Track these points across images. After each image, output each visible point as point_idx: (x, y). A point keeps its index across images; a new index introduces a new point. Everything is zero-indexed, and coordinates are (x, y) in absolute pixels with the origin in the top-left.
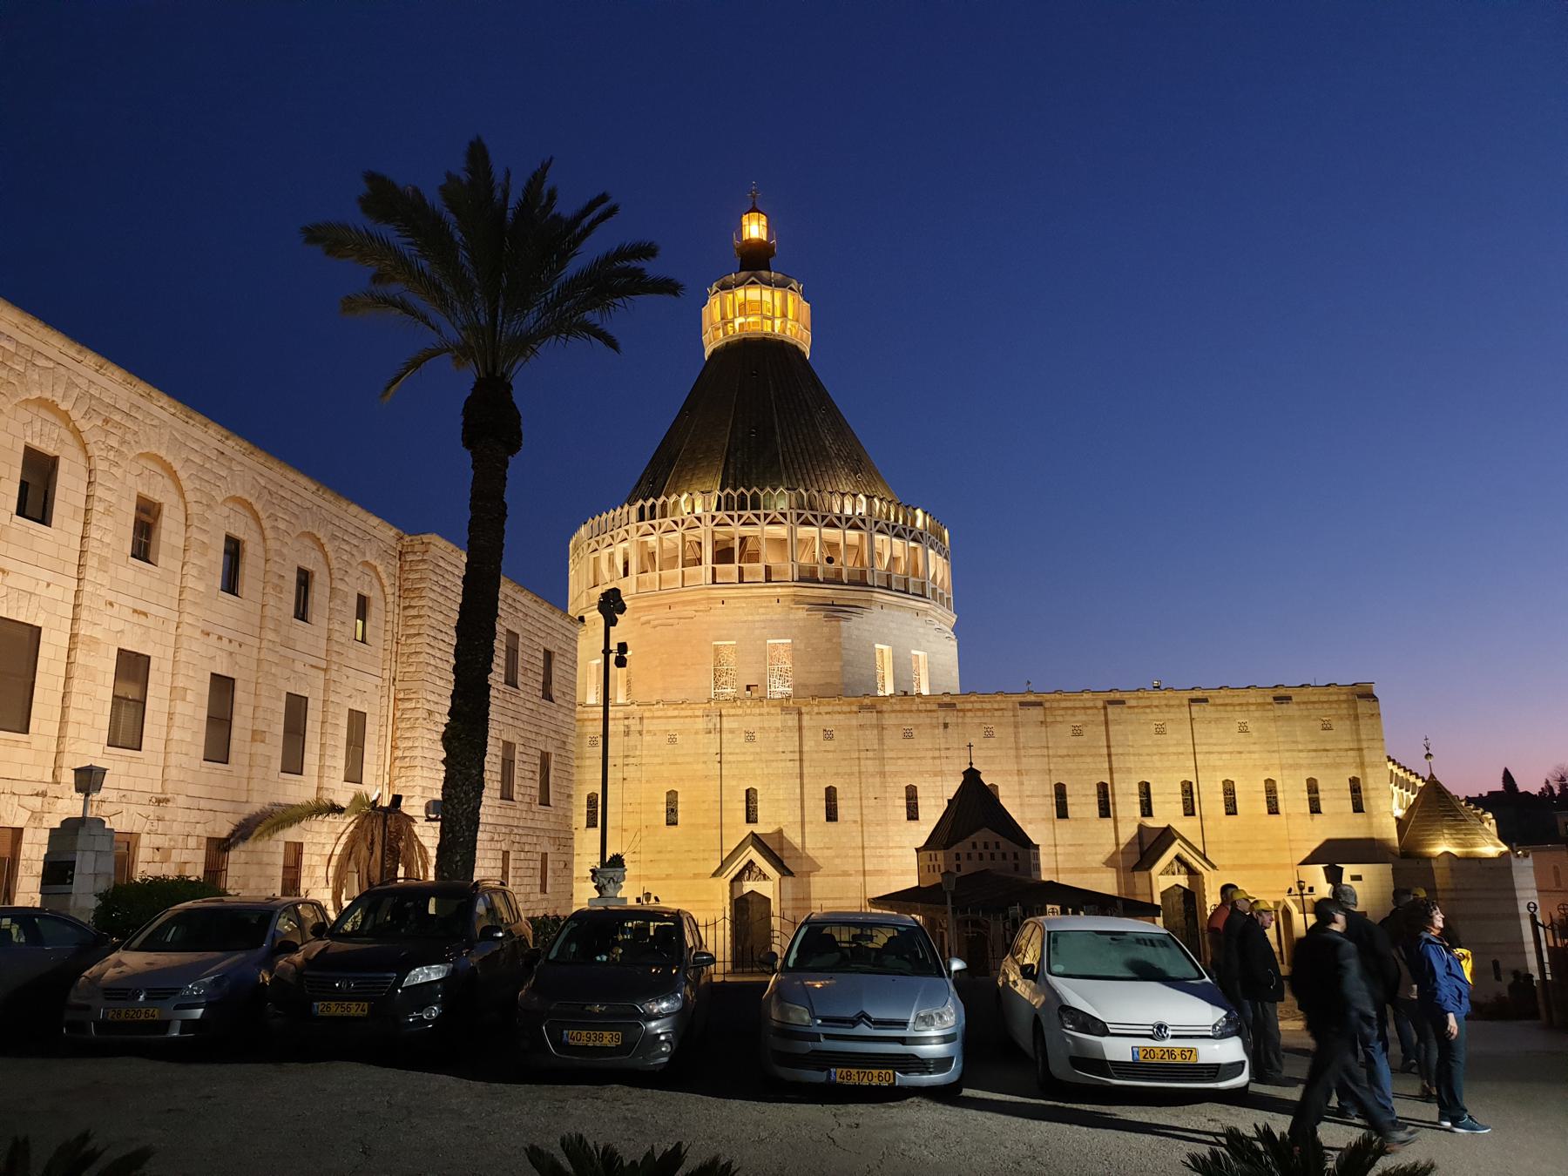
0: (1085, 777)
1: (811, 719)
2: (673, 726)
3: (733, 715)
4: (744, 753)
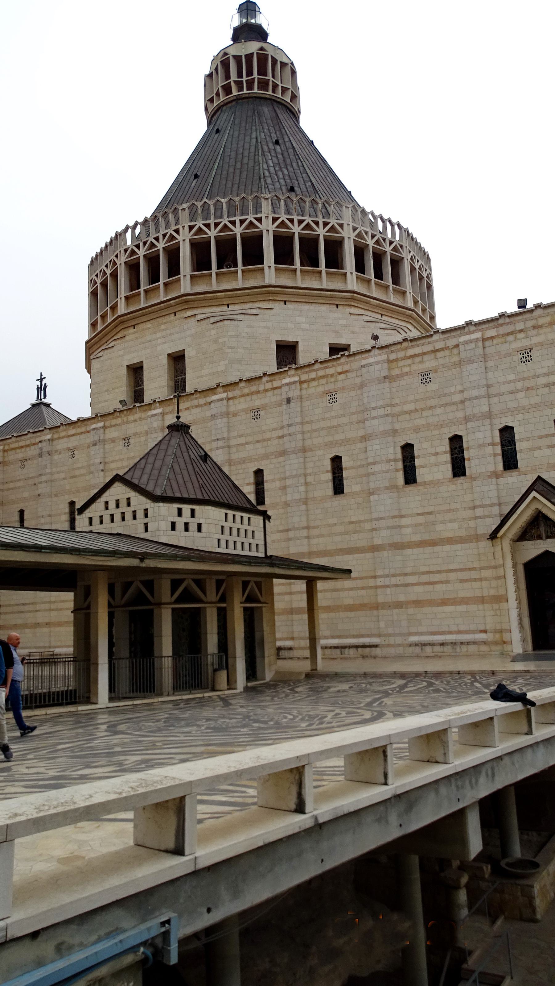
0: (436, 432)
2: (73, 442)
3: (114, 426)
4: (121, 460)
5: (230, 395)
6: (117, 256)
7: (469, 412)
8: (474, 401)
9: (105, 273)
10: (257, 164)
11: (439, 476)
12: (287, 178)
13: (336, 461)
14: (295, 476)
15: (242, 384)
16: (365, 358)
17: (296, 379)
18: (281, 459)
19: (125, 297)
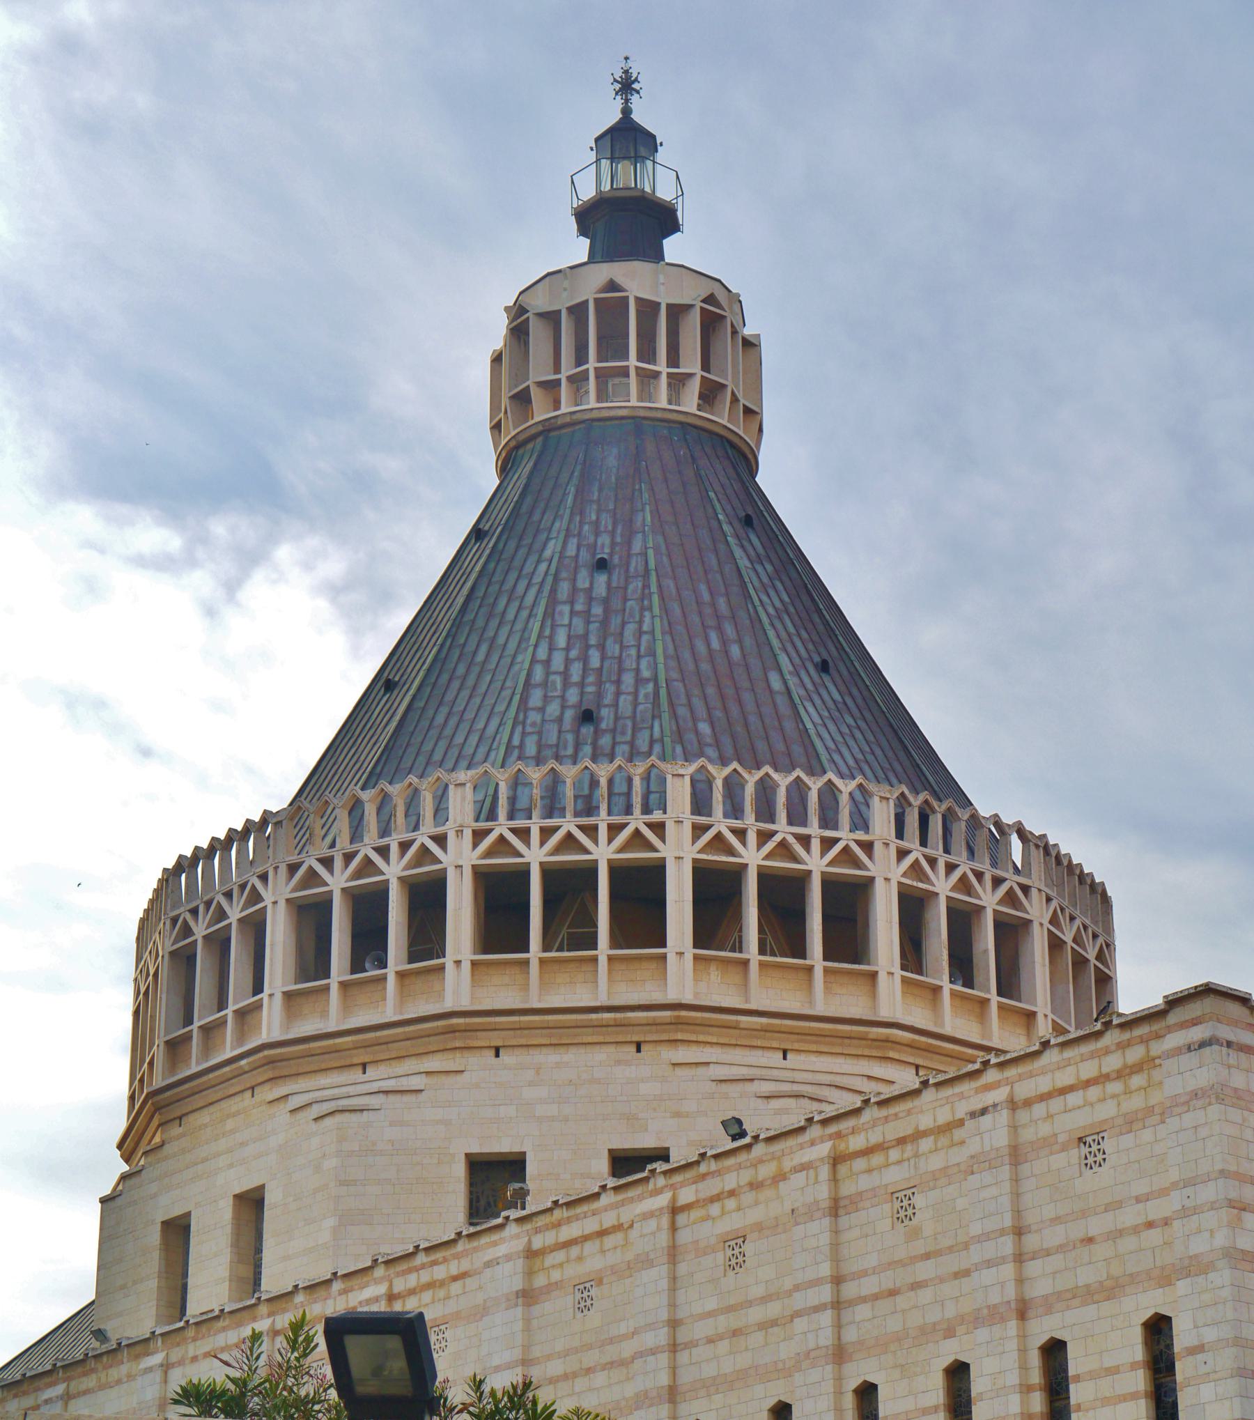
16: (495, 1244)
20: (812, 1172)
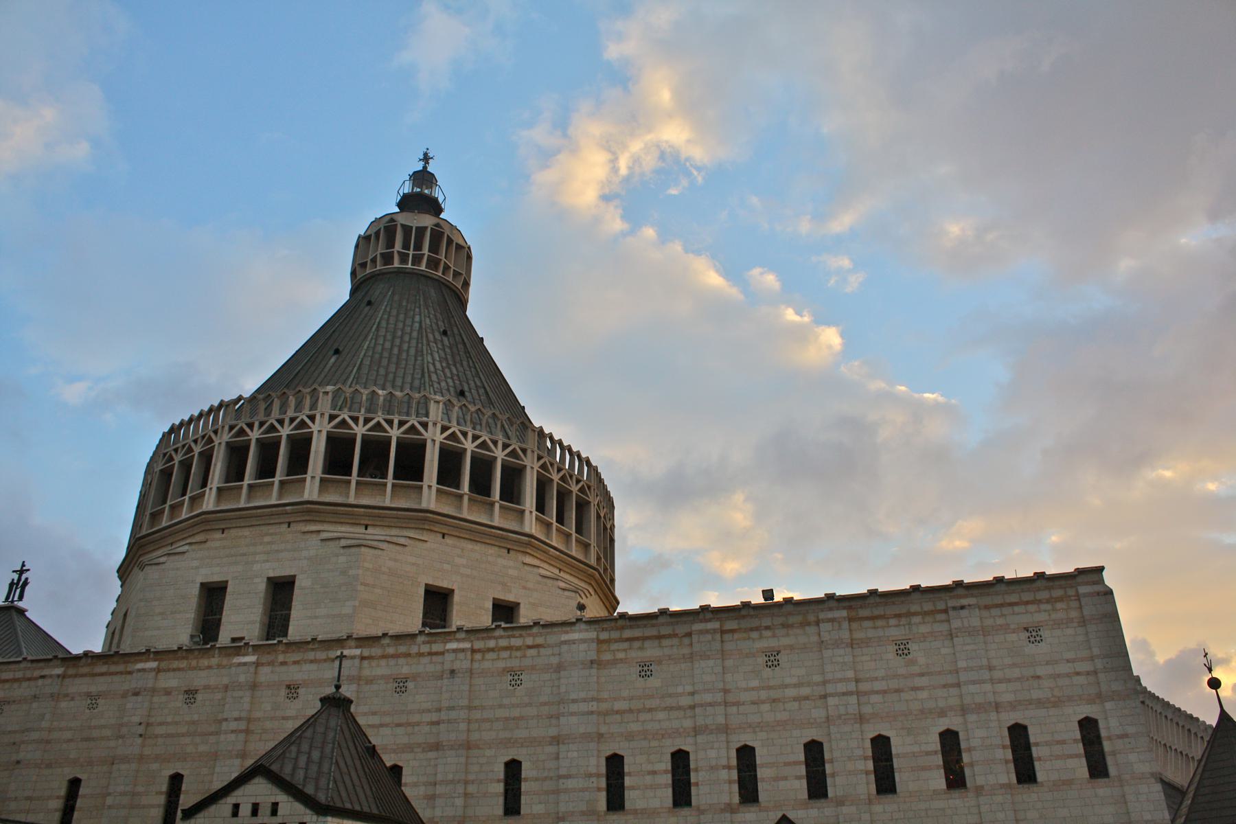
1: (272, 672)
2: (100, 685)
4: (176, 723)
5: (366, 653)
6: (216, 432)
7: (700, 721)
8: (708, 708)
9: (190, 450)
10: (419, 354)
11: (655, 803)
12: (455, 378)
13: (513, 768)
14: (452, 782)
15: (386, 641)
16: (567, 632)
17: (467, 645)
18: (432, 755)
19: (218, 488)
20: (836, 624)
